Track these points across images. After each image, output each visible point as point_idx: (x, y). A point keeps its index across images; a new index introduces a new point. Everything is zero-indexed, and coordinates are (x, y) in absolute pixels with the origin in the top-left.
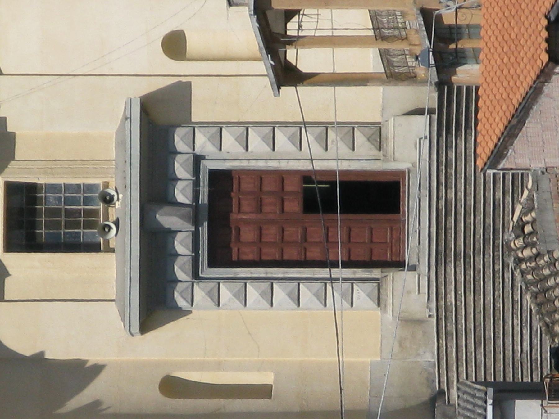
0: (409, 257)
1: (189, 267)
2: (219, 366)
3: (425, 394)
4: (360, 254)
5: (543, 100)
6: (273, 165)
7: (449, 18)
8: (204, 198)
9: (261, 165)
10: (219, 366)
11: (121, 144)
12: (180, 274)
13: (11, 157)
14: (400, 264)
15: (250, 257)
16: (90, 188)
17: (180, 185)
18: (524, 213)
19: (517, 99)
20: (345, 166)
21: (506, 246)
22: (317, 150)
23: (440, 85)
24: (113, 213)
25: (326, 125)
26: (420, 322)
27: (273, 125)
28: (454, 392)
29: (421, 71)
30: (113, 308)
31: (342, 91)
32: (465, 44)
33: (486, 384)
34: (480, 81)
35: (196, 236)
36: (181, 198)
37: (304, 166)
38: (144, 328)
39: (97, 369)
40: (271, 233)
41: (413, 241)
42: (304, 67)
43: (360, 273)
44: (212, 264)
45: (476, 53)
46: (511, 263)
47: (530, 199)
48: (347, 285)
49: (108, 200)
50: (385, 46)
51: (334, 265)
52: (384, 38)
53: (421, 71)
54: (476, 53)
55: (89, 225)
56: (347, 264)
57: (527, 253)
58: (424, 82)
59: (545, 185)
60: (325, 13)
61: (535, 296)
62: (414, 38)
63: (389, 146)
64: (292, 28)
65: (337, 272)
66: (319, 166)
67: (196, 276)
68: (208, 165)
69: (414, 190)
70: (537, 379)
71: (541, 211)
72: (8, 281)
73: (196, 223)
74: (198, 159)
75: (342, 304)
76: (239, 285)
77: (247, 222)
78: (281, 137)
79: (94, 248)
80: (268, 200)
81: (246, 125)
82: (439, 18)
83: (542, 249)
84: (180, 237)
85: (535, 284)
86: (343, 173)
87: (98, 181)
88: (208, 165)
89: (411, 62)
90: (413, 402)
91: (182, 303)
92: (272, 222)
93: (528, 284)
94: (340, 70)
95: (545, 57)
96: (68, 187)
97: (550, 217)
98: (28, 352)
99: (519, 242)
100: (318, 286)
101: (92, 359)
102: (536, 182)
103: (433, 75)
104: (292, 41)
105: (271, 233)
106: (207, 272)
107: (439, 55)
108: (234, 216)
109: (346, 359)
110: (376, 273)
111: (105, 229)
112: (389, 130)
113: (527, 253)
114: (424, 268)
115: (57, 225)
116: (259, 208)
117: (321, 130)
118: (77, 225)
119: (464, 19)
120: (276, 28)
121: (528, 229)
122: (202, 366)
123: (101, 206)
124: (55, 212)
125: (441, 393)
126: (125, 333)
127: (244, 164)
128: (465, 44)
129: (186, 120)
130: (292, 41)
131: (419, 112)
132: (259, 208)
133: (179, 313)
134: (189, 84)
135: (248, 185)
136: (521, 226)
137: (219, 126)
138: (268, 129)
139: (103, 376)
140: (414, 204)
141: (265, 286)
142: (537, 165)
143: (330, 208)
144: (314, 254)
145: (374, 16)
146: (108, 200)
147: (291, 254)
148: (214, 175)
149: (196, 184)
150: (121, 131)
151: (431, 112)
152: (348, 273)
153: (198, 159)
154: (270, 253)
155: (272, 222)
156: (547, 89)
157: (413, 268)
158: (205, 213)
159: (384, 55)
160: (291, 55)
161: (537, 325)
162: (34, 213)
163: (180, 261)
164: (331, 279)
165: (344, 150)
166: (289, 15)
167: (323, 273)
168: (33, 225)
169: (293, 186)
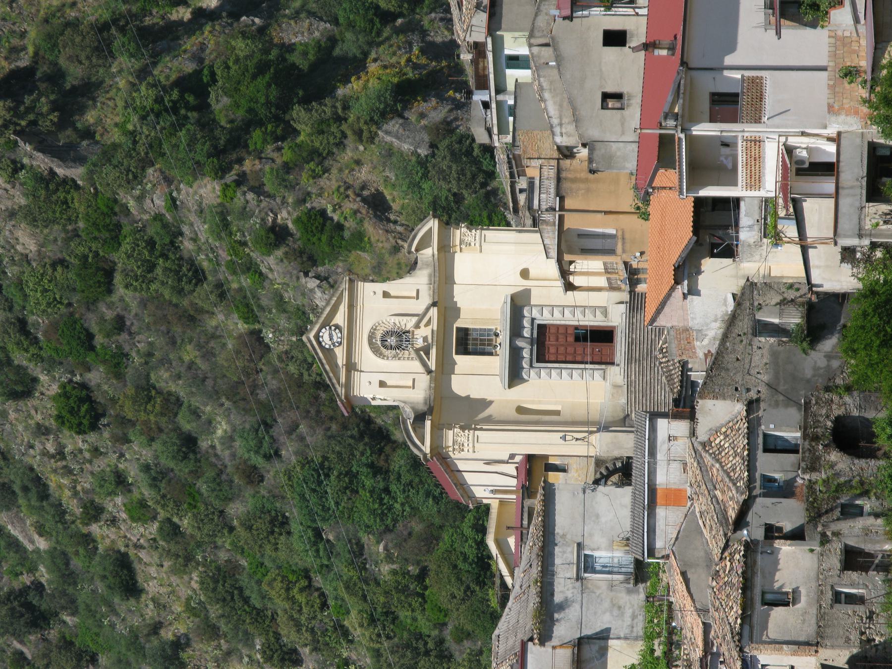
0: (617, 361)
1: (529, 363)
2: (540, 402)
3: (622, 415)
4: (597, 359)
5: (672, 299)
6: (563, 323)
7: (635, 265)
8: (535, 335)
9: (558, 322)
10: (540, 402)
11: (502, 312)
12: (525, 365)
13: (459, 317)
14: (613, 363)
15: (553, 359)
16: (490, 330)
17: (526, 330)
18: (663, 344)
19: (661, 298)
20: (592, 324)
21: (656, 357)
22: (581, 317)
23: (630, 292)
24: (499, 340)
25: (585, 307)
26: (620, 386)
27: (564, 307)
28: (633, 415)
29: (623, 286)
30: (498, 378)
31: (591, 293)
32: (641, 276)
33: (646, 412)
34: (646, 291)
35: (531, 350)
36: (526, 335)
37: (576, 323)
38: (510, 386)
39: (491, 402)
40: (562, 350)
41: (618, 354)
42: (576, 284)
43: (597, 366)
44: (538, 361)
45: (645, 280)
46: (657, 363)
47: (666, 338)
48: (591, 371)
49: (497, 335)
50: (609, 276)
51: (586, 363)
52: (609, 273)
53: (623, 286)
54: (645, 280)
55: (489, 345)
56: (592, 363)
57: (664, 360)
58: (624, 291)
59: (672, 333)
60: (585, 262)
61: (666, 377)
62: (621, 273)
63: (610, 316)
64: (572, 268)
65: (587, 366)
66: (581, 323)
67: (531, 366)
68: (537, 322)
69: (619, 334)
70: (667, 410)
71: (670, 343)
72: (456, 366)
73: (532, 345)
74: (533, 320)
75: (589, 378)
76: (548, 370)
77: (552, 345)
78: (567, 311)
79: (491, 354)
80: (560, 336)
81: (553, 306)
82: (631, 265)
83: (670, 358)
84: (525, 350)
85: (667, 372)
86: (591, 326)
87: (493, 327)
88: (537, 322)
89: (619, 283)
90: (617, 419)
91: (525, 377)
92: (562, 345)
93: (664, 372)
94: (590, 285)
95: (673, 282)
96: (481, 329)
97: (673, 346)
98: (463, 395)
99: (661, 356)
100: (580, 371)
101: (489, 398)
102: (668, 332)
103: (628, 288)
104: (572, 273)
105: (562, 350)
106: (536, 365)
107: (630, 280)
108: (547, 343)
109: (591, 401)
110: (603, 367)
111: (495, 346)
112: (610, 310)
113: (664, 360)
114: (622, 365)
115: (476, 344)
116: (557, 340)
117: (582, 309)
118: (484, 345)
119: (640, 266)
120: (566, 268)
121: (664, 350)
122: (533, 402)
123: (494, 337)
124: (476, 339)
125: (628, 415)
126: (502, 388)
127: (552, 322)
128: (641, 276)
129: (529, 304)
130: (572, 273)
131: (622, 303)
132: (557, 340)
133: (525, 381)
134: (530, 290)
135: (553, 331)
136: (661, 349)
137: (542, 307)
138: (561, 309)
139: (493, 405)
140: (619, 339)
141: (559, 370)
142: (669, 325)
143: (585, 339)
144: (579, 358)
145: (605, 264)
146: (497, 335)
147: (569, 358)
148: (539, 325)
149: (532, 329)
150: (503, 307)
151: (627, 303)
152: (592, 366)
153: (533, 320)
154: (561, 358)
155: (562, 345)
156: (673, 294)
157: (618, 365)
158: (535, 341)
159: (608, 279)
160: (571, 278)
161: (667, 389)
162: (467, 339)
163: (525, 360)
164: (585, 369)
165: (591, 317)
166: (571, 262)
167: (582, 366)
168: (467, 344)
169: (570, 331)
